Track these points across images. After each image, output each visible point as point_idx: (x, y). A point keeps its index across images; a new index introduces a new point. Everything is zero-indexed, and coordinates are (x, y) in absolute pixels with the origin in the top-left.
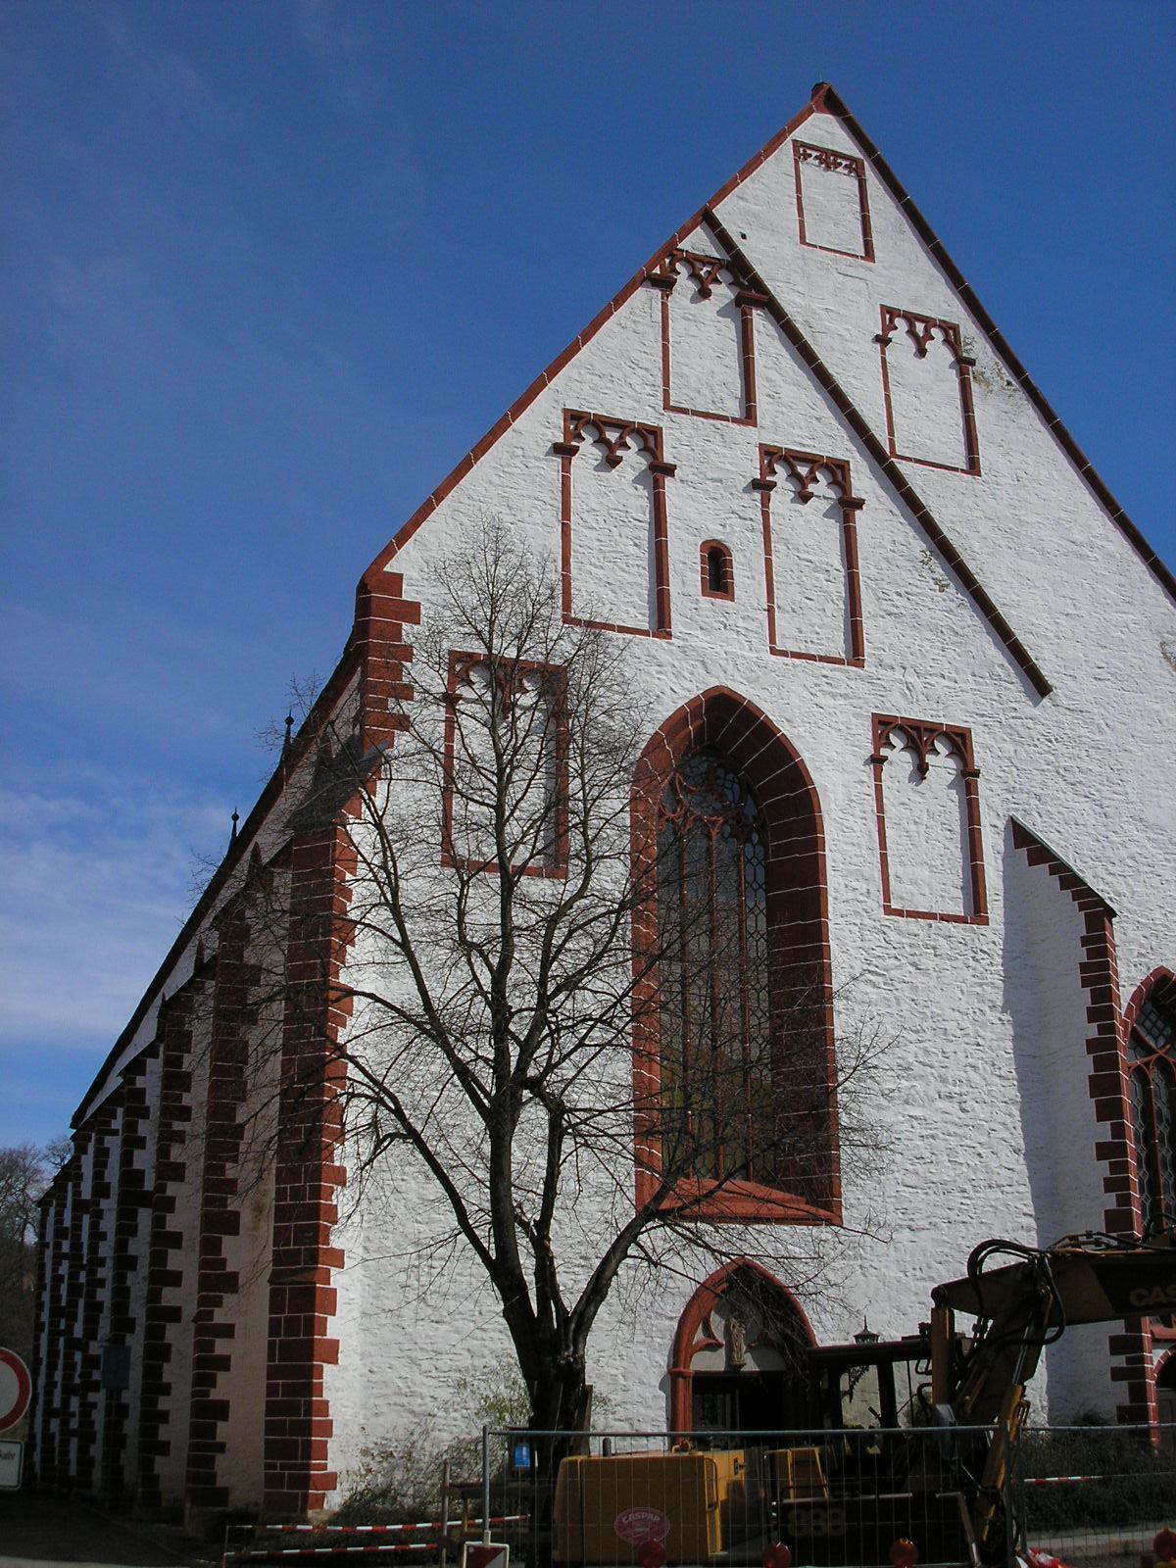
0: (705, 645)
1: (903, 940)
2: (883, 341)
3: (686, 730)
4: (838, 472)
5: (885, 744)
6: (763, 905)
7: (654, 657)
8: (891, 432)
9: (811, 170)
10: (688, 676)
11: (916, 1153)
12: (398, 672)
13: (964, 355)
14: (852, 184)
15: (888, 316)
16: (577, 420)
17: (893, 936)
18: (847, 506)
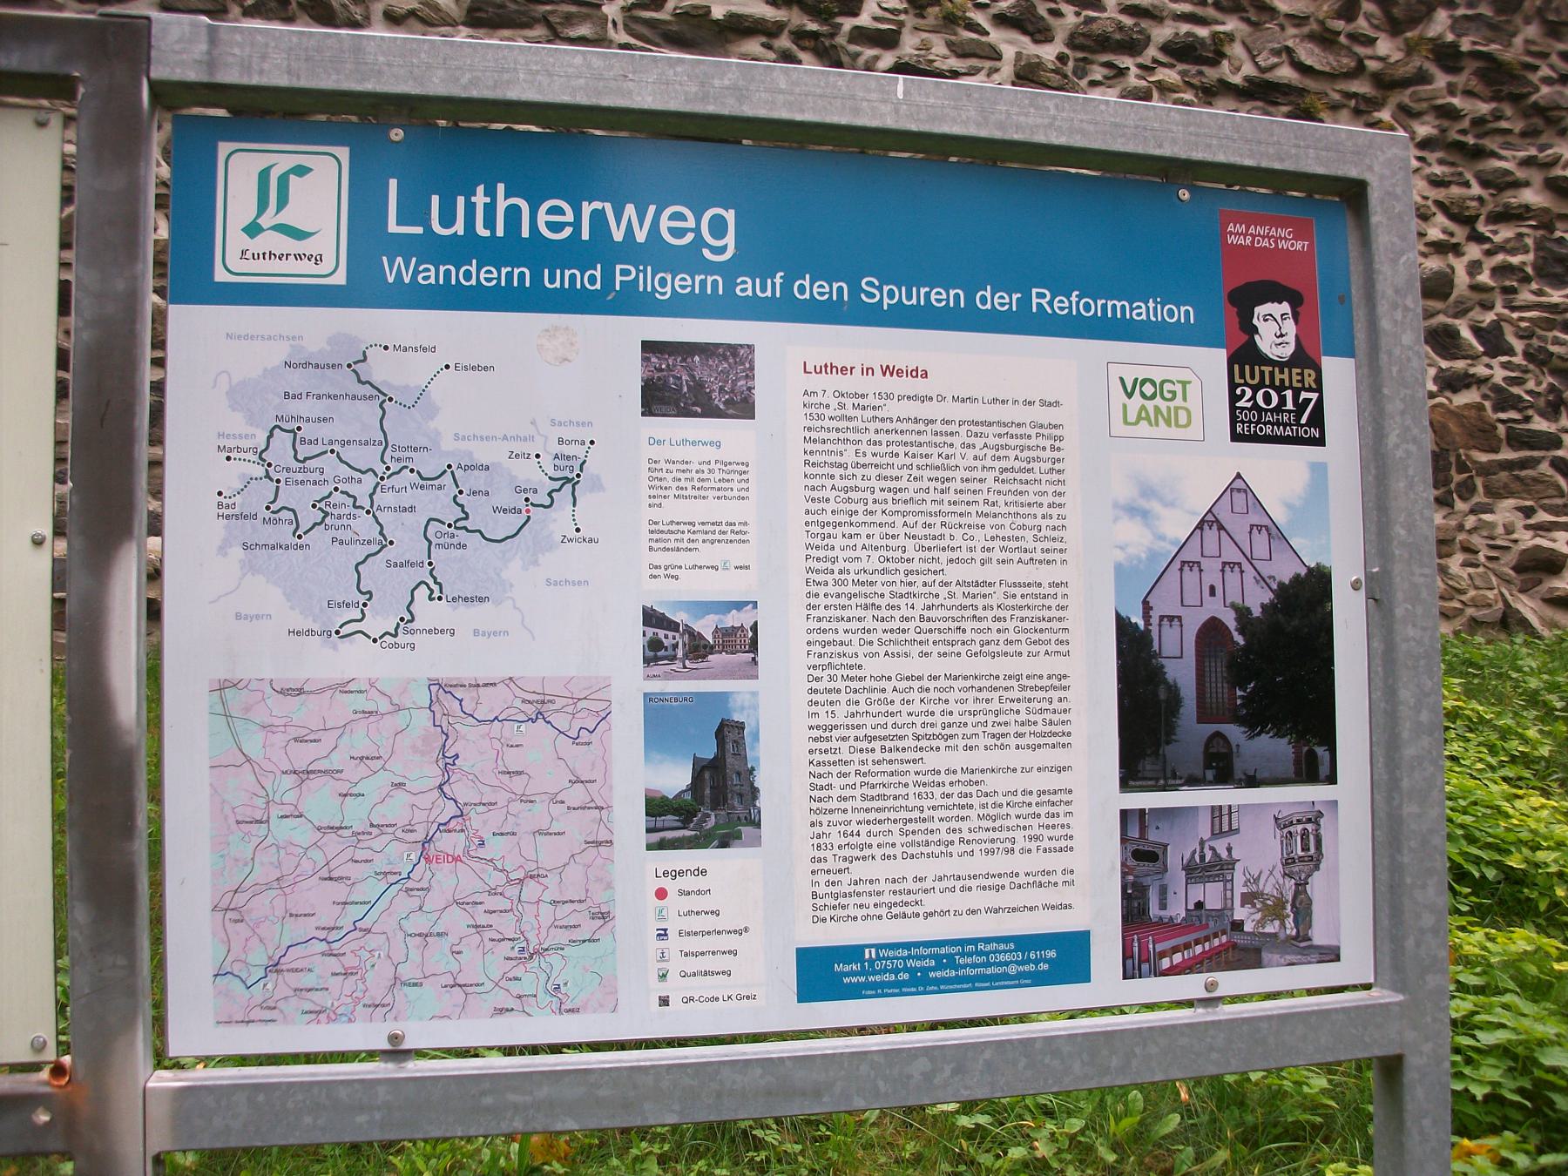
4: (1239, 564)
9: (1235, 494)
16: (1183, 563)
18: (1242, 572)
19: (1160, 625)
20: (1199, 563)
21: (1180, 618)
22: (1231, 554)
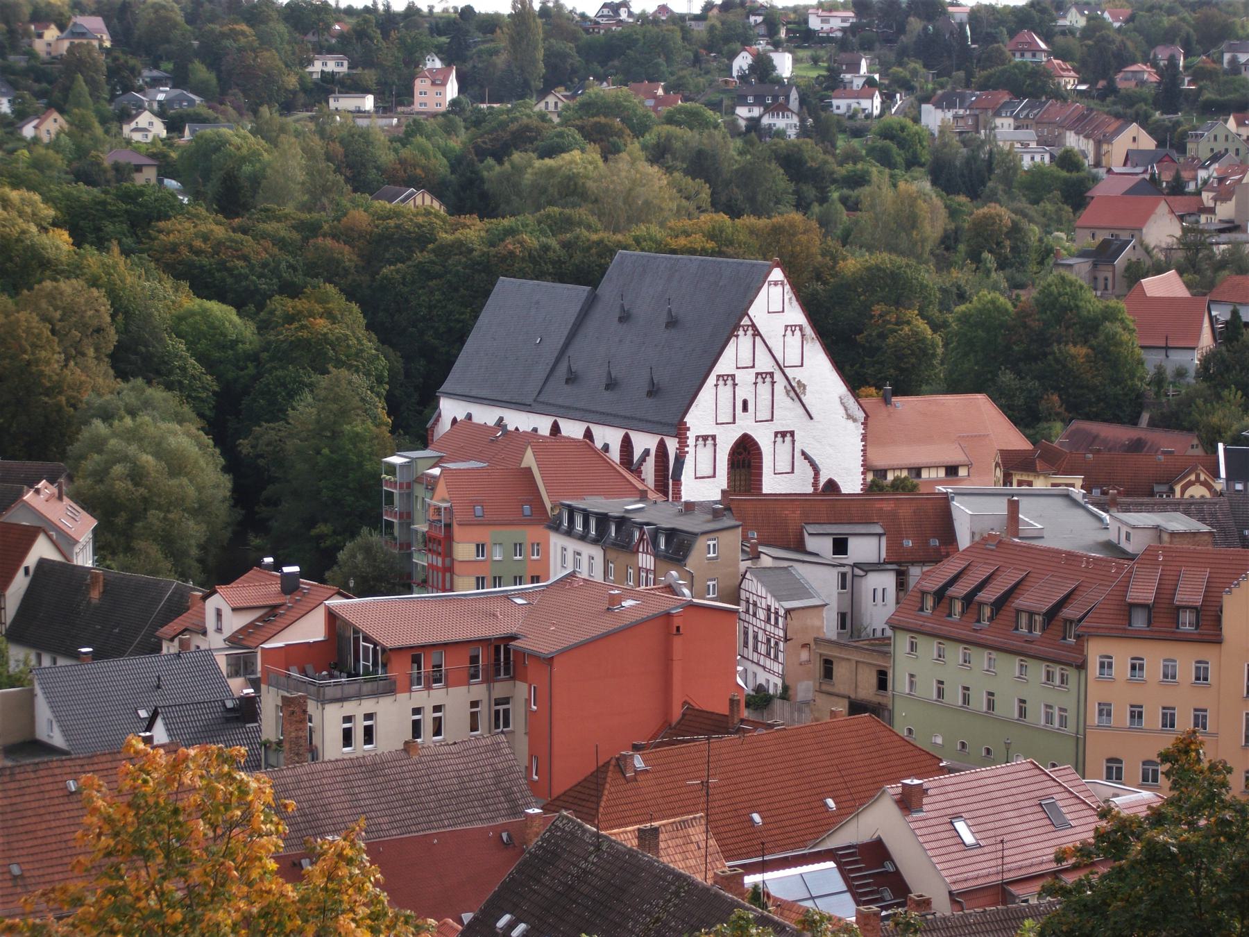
4: (772, 374)
9: (772, 288)
16: (718, 377)
21: (714, 437)
22: (764, 364)
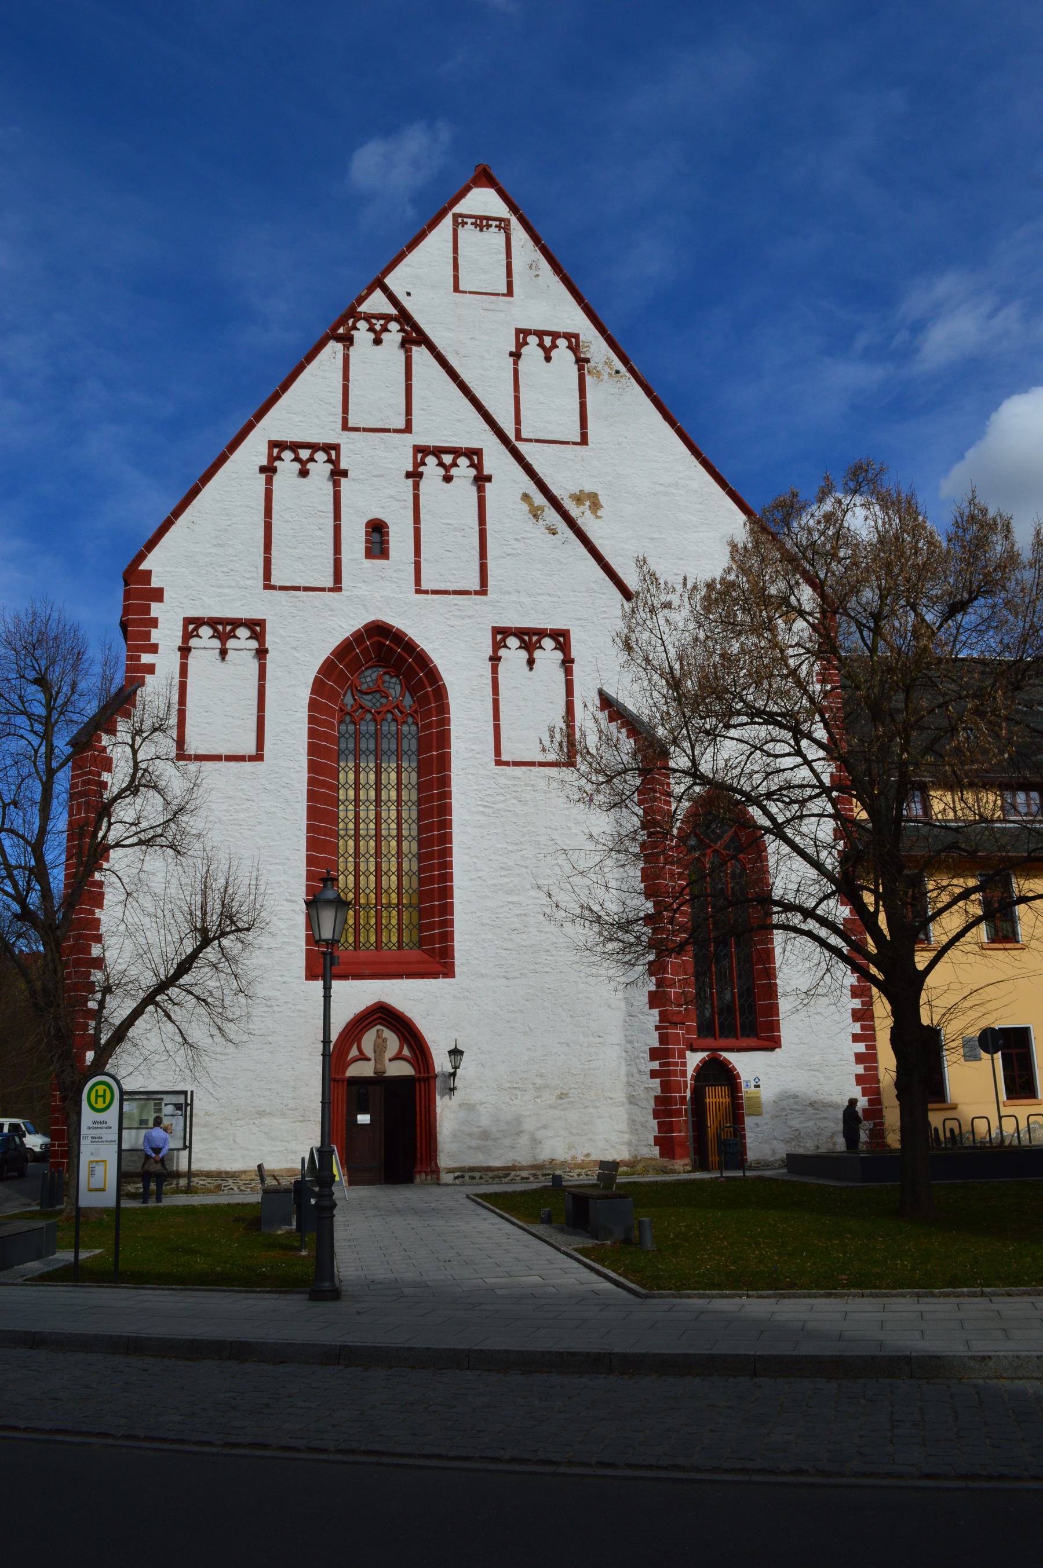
0: (367, 593)
1: (508, 782)
2: (516, 355)
3: (354, 653)
4: (474, 455)
5: (503, 647)
6: (414, 765)
7: (328, 605)
8: (518, 421)
9: (468, 234)
10: (352, 615)
11: (513, 927)
12: (147, 635)
13: (582, 356)
14: (497, 238)
15: (522, 336)
16: (273, 444)
17: (502, 781)
18: (481, 480)
19: (185, 651)
20: (331, 449)
21: (257, 628)
